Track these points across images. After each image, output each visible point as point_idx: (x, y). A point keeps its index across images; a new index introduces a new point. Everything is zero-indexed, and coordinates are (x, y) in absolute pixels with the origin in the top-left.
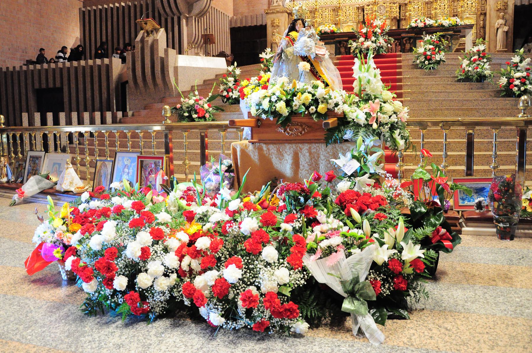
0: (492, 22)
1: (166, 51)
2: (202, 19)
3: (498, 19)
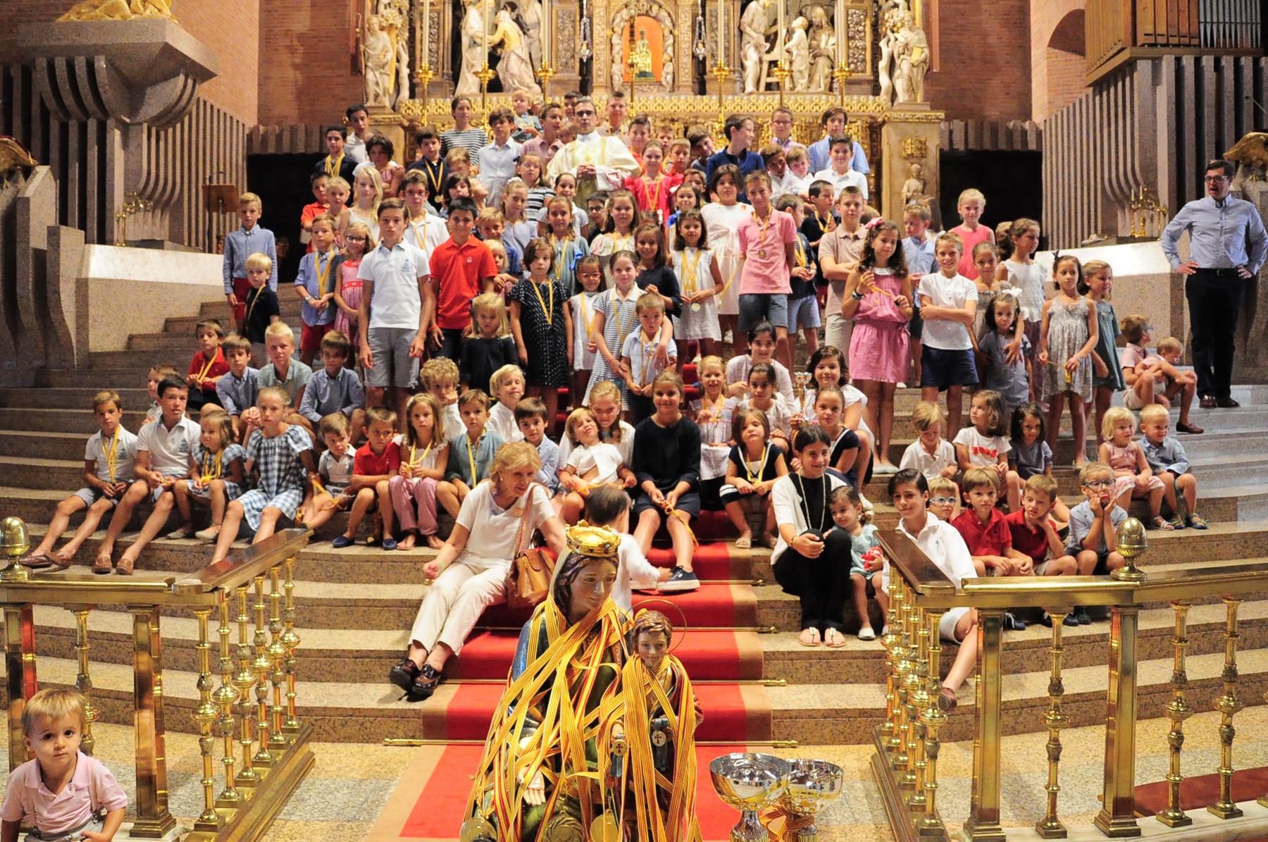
0: (896, 182)
1: (53, 234)
2: (170, 130)
3: (908, 178)
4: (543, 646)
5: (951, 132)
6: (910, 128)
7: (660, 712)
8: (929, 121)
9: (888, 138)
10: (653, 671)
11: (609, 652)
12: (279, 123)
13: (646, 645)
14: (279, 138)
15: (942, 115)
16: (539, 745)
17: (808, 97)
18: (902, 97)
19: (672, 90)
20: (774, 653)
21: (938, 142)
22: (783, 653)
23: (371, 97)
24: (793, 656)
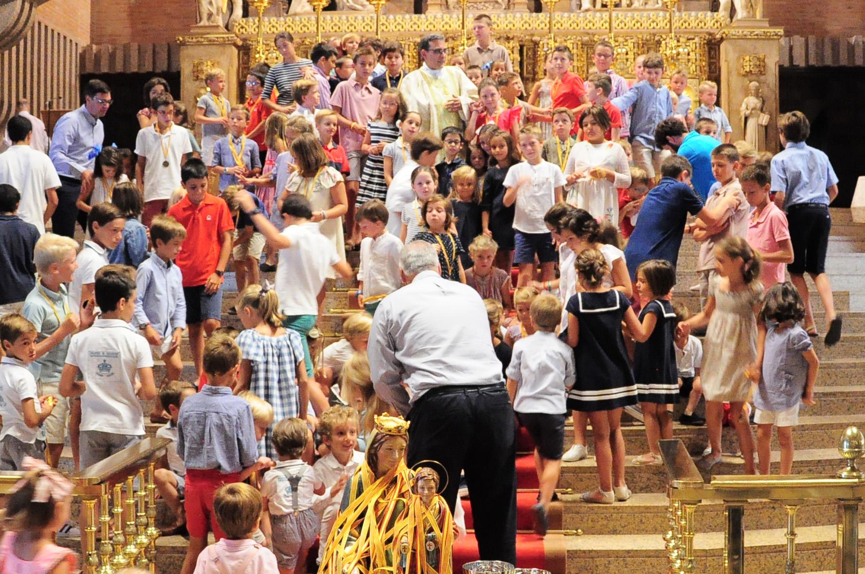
0: (734, 101)
2: (6, 53)
3: (747, 96)
4: (360, 492)
5: (791, 49)
6: (748, 45)
7: (431, 530)
8: (768, 38)
9: (726, 55)
10: (427, 505)
11: (402, 495)
12: (113, 42)
13: (423, 488)
14: (112, 56)
15: (781, 31)
16: (356, 551)
17: (645, 14)
18: (740, 14)
19: (508, 8)
20: (576, 552)
21: (777, 59)
22: (584, 552)
23: (205, 16)
24: (592, 554)
